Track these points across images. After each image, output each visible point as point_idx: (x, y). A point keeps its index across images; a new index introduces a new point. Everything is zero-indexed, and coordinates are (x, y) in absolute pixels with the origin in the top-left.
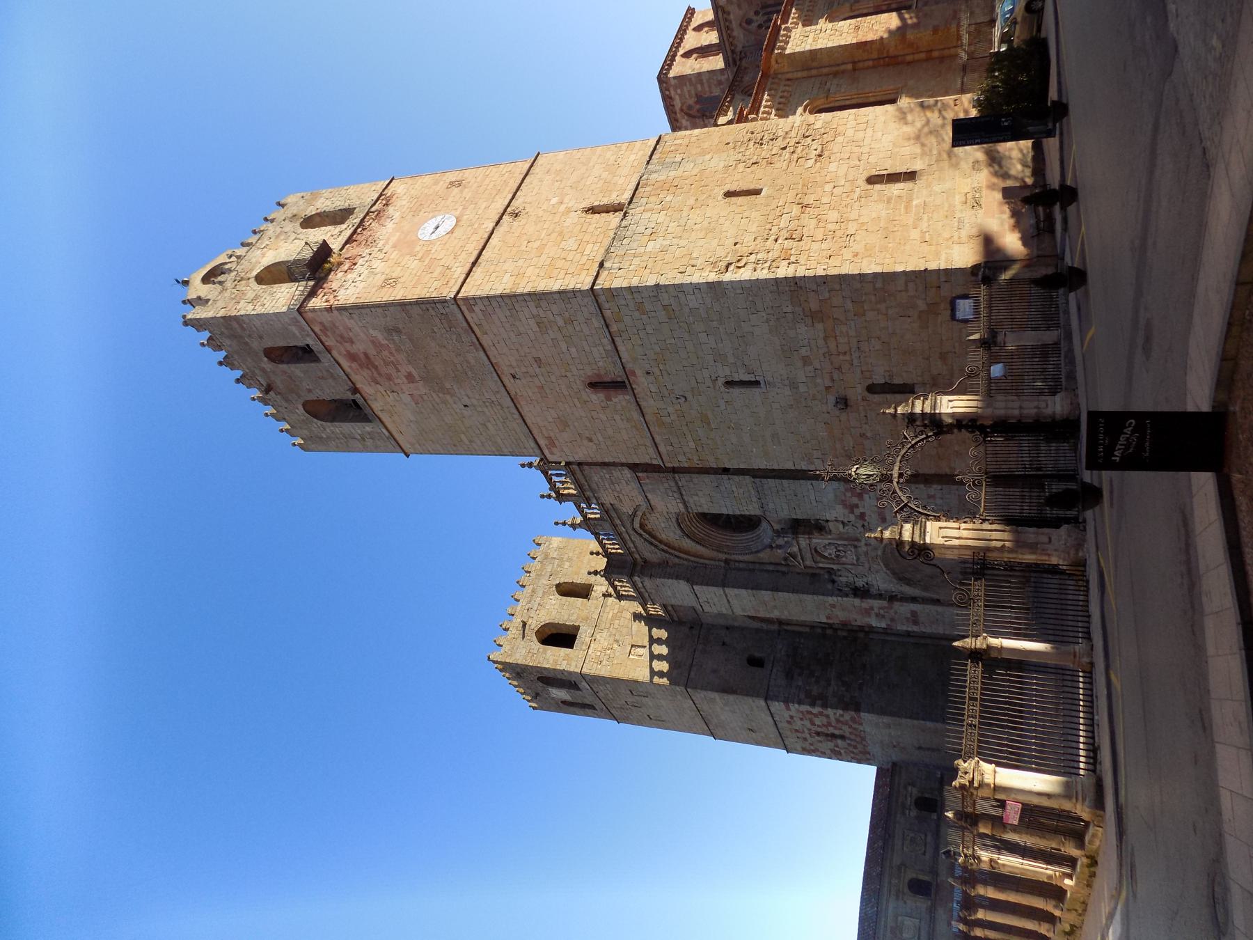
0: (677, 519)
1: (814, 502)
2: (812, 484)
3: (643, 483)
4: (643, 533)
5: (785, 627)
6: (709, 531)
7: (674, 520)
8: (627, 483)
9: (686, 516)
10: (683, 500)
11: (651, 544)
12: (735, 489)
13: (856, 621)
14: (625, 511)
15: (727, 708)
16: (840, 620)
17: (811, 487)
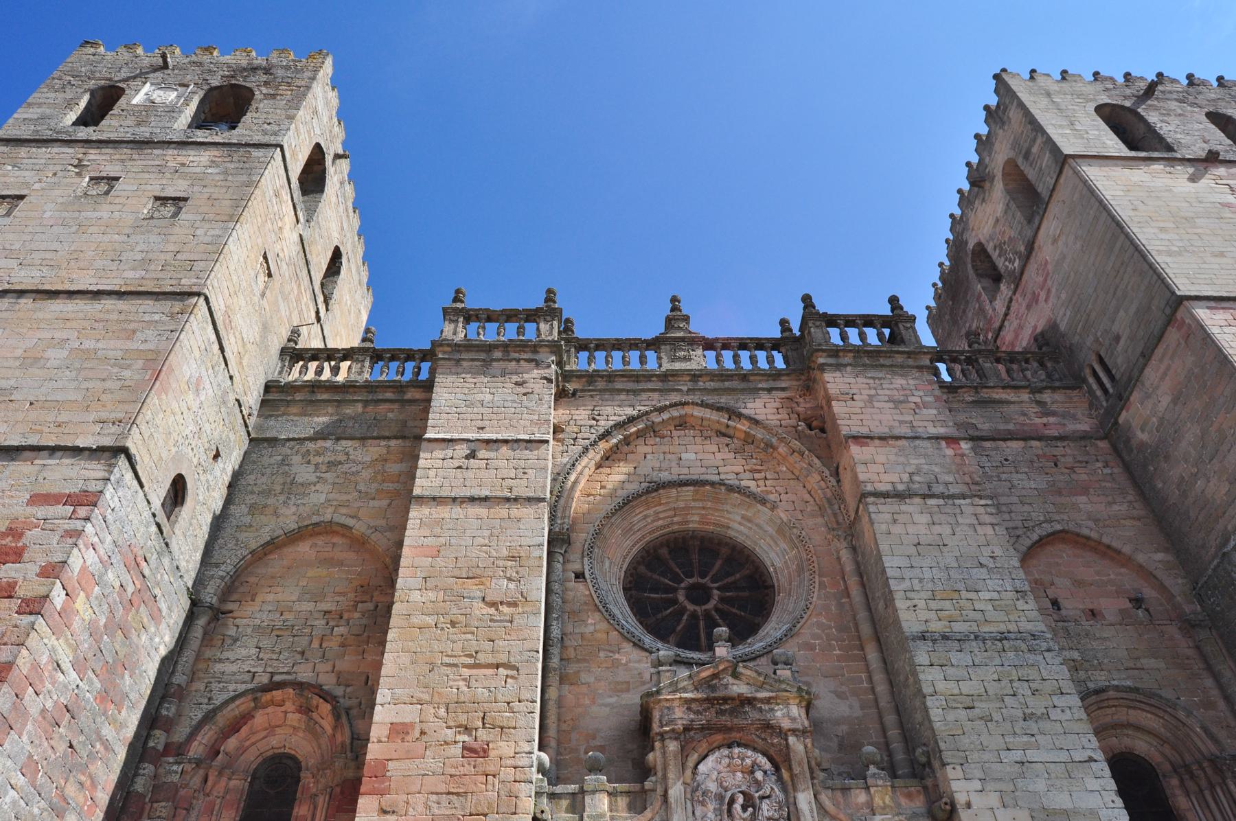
0: (712, 484)
1: (1018, 755)
2: (1091, 760)
3: (939, 443)
4: (665, 416)
5: (201, 622)
6: (639, 535)
7: (716, 478)
8: (906, 422)
9: (709, 504)
10: (911, 496)
11: (631, 420)
12: (985, 595)
13: (385, 812)
14: (749, 405)
15: (56, 356)
16: (382, 764)
17: (1079, 756)
